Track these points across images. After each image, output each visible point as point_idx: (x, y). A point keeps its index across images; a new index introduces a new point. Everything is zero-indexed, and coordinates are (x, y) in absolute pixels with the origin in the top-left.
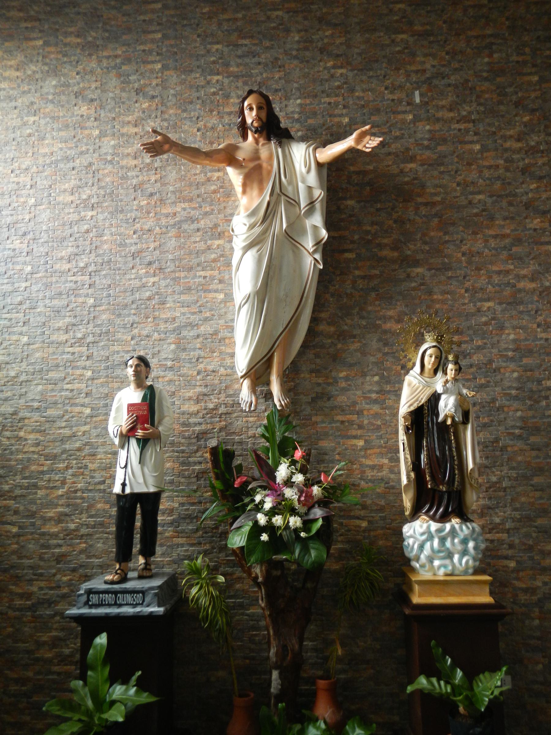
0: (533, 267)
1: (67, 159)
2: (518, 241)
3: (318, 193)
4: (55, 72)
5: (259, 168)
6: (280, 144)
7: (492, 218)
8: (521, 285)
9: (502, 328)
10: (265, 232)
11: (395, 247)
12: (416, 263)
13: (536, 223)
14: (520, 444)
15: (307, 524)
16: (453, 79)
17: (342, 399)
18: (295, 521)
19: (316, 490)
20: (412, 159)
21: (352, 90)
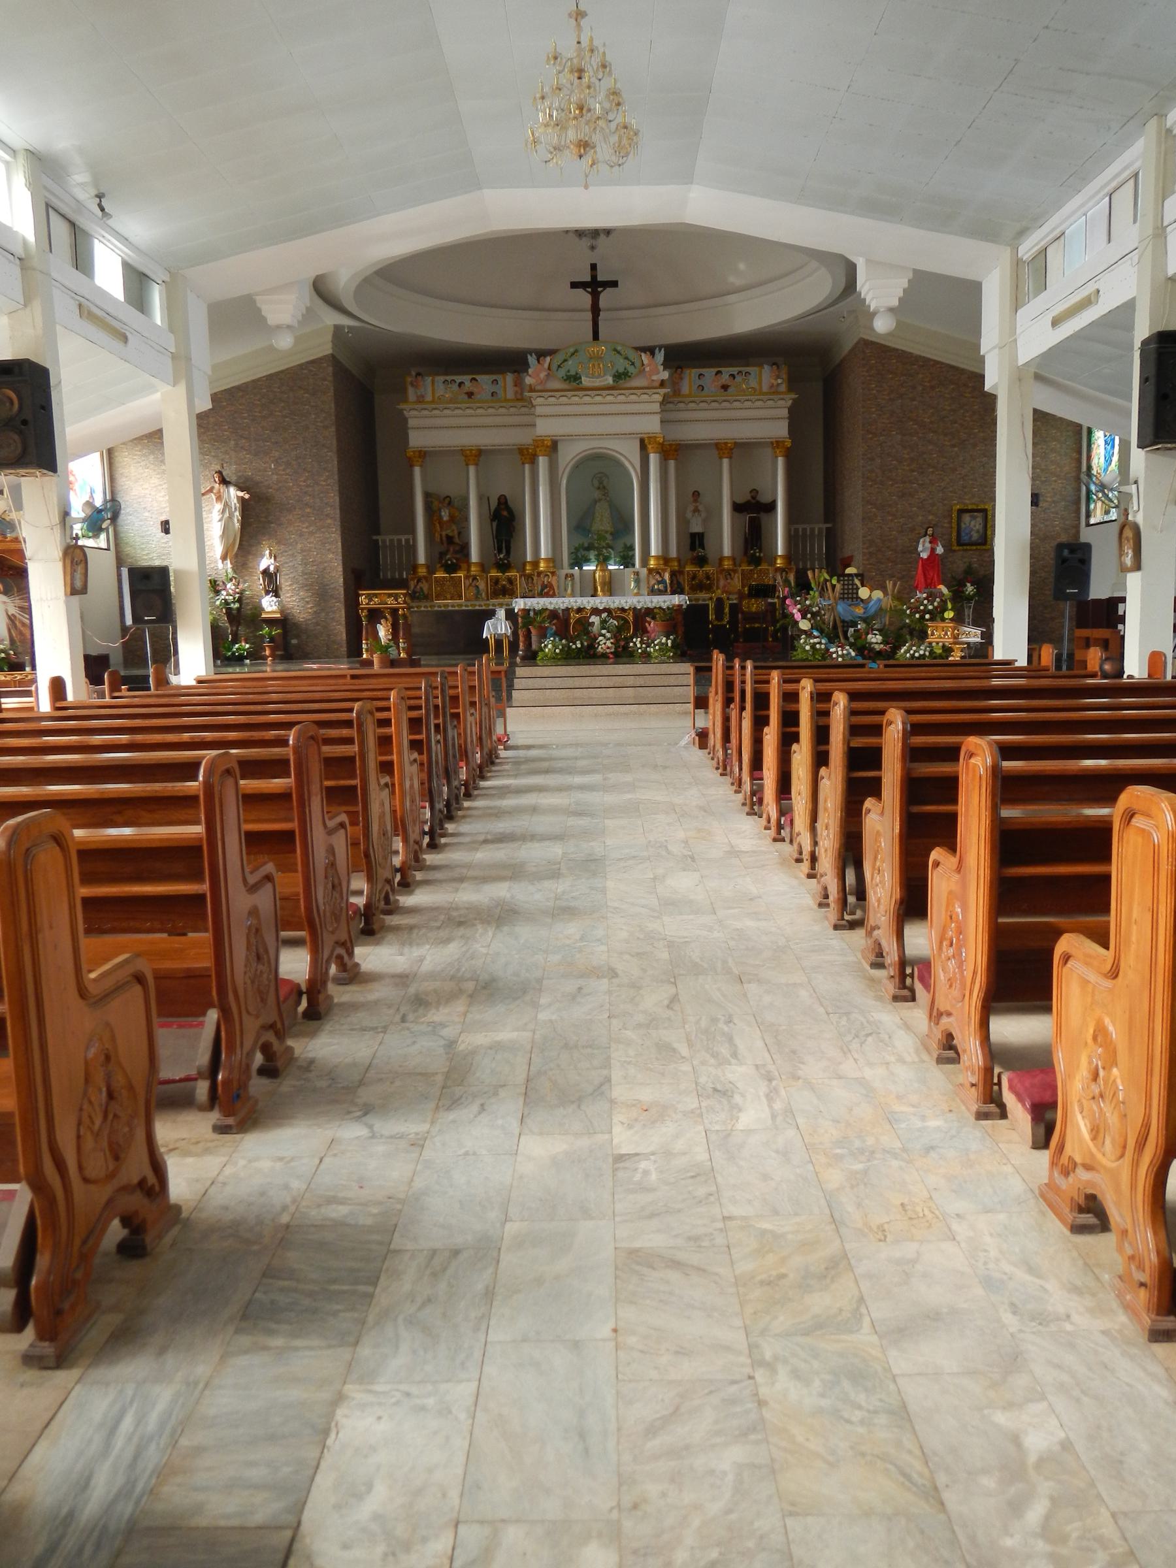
0: (307, 524)
1: (160, 485)
2: (303, 516)
3: (238, 505)
4: (152, 453)
5: (220, 496)
6: (227, 487)
7: (295, 508)
8: (303, 530)
9: (297, 543)
10: (222, 517)
11: (266, 517)
12: (272, 523)
13: (308, 510)
14: (301, 578)
15: (234, 598)
16: (284, 460)
17: (251, 565)
18: (231, 598)
19: (237, 590)
20: (271, 488)
21: (252, 463)
